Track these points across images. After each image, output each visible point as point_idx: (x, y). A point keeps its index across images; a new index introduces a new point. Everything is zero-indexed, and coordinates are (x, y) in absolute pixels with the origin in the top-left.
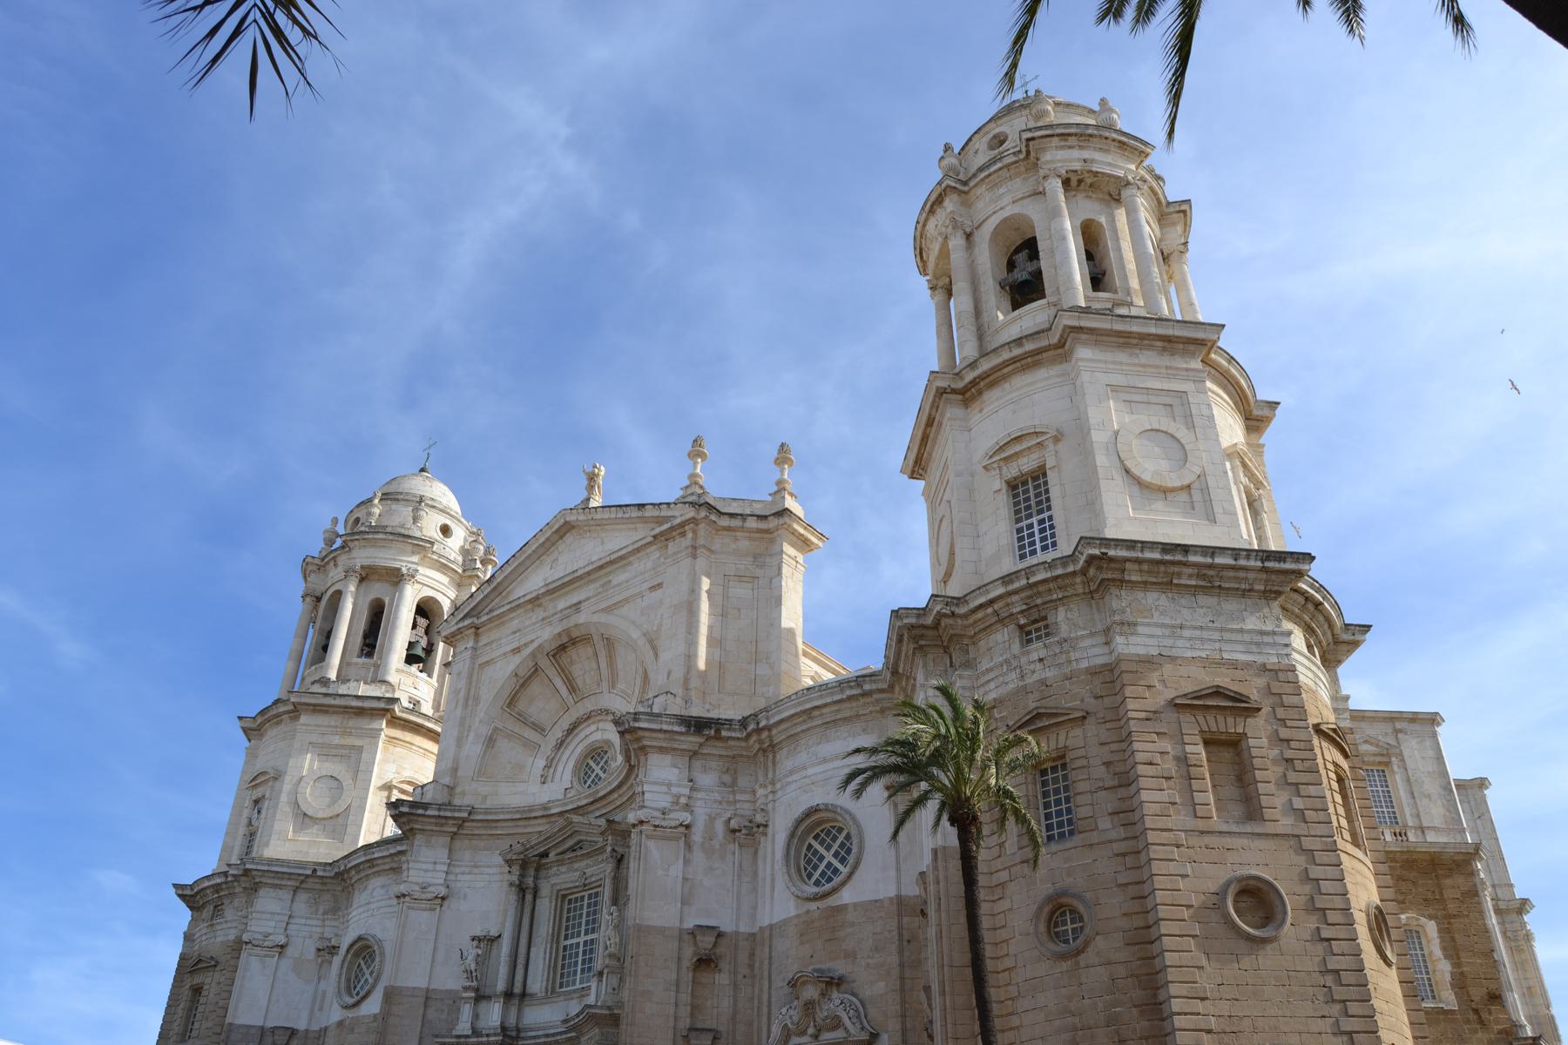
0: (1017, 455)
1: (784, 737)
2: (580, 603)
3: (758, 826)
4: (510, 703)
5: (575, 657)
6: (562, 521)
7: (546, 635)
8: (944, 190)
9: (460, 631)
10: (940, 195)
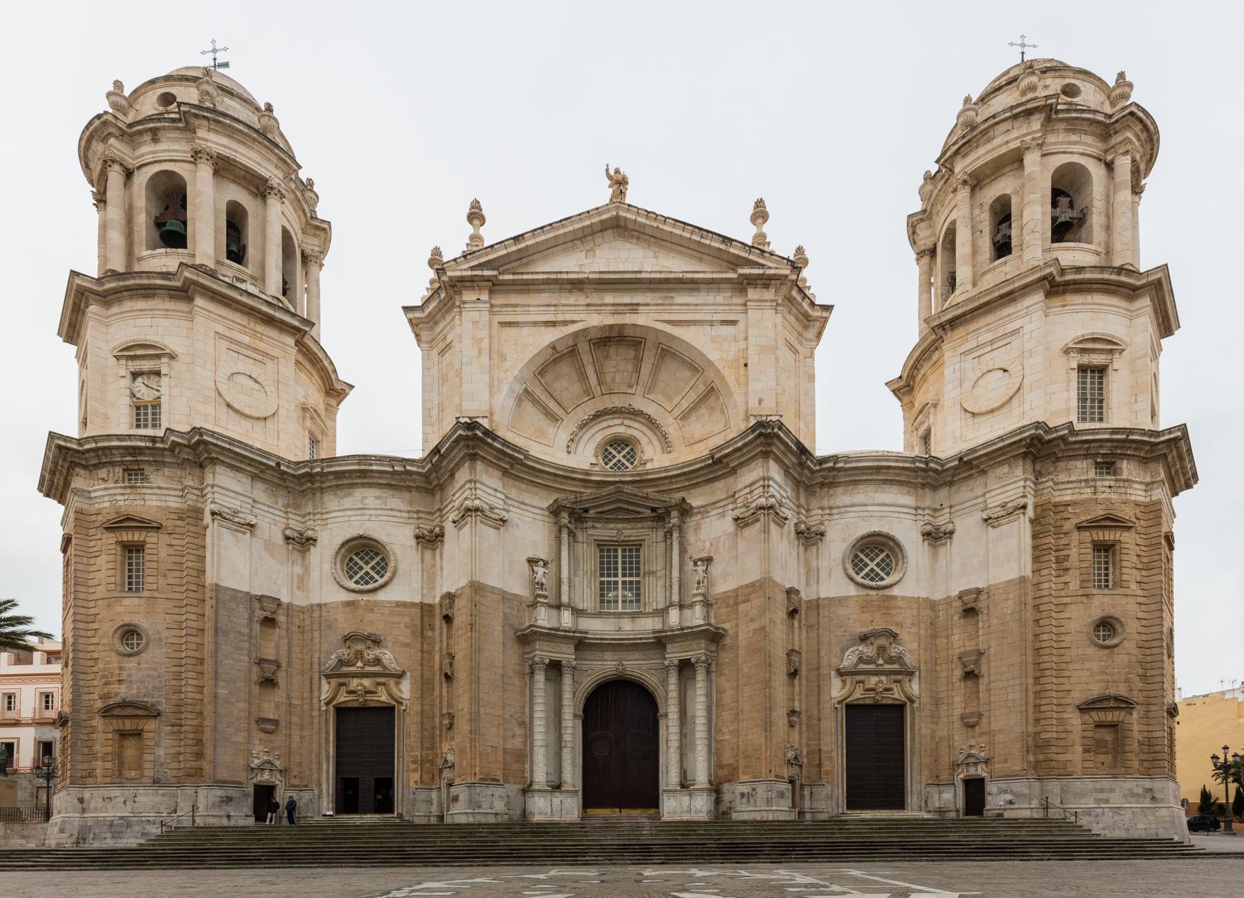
2: (638, 305)
6: (614, 213)
7: (595, 320)
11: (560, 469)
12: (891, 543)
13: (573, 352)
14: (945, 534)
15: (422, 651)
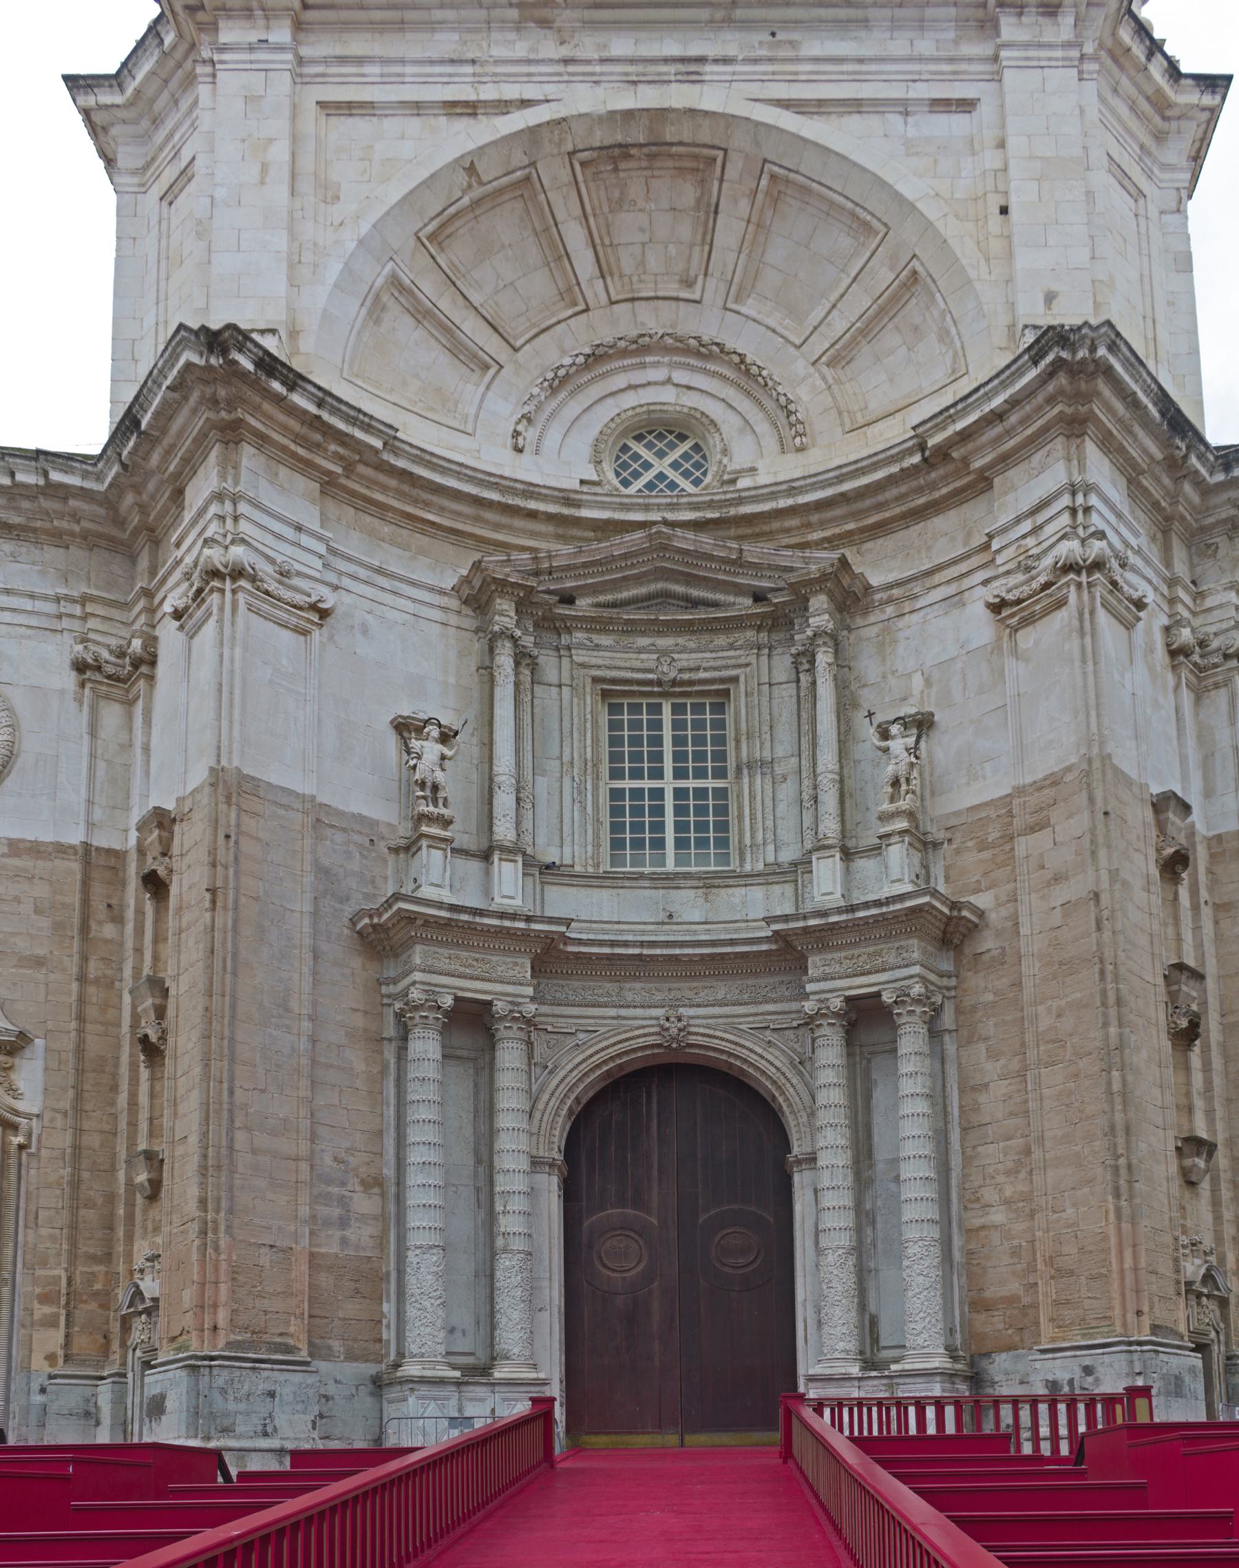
2: (701, 60)
5: (635, 189)
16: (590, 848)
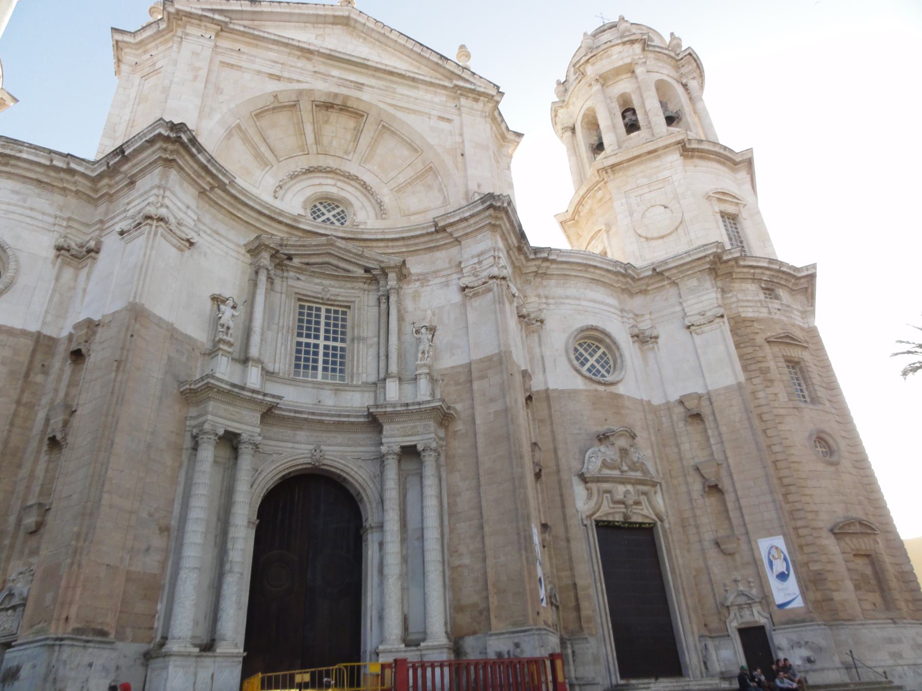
0: (725, 201)
1: (558, 273)
2: (363, 84)
3: (537, 321)
4: (256, 115)
6: (346, 14)
7: (322, 87)
8: (641, 40)
9: (201, 18)
10: (637, 40)
11: (268, 208)
12: (608, 340)
13: (294, 106)
14: (651, 338)
15: (18, 402)
16: (287, 366)
